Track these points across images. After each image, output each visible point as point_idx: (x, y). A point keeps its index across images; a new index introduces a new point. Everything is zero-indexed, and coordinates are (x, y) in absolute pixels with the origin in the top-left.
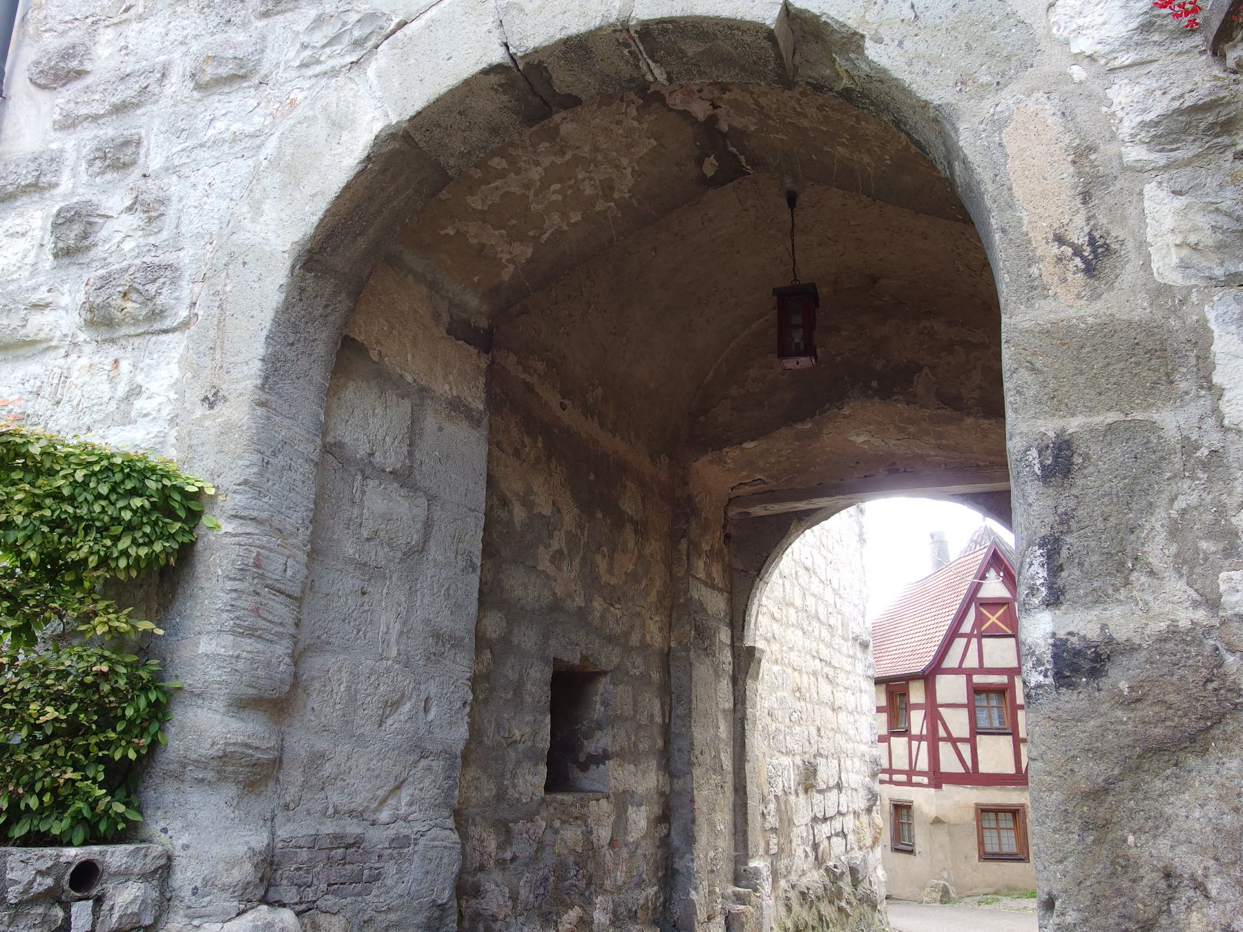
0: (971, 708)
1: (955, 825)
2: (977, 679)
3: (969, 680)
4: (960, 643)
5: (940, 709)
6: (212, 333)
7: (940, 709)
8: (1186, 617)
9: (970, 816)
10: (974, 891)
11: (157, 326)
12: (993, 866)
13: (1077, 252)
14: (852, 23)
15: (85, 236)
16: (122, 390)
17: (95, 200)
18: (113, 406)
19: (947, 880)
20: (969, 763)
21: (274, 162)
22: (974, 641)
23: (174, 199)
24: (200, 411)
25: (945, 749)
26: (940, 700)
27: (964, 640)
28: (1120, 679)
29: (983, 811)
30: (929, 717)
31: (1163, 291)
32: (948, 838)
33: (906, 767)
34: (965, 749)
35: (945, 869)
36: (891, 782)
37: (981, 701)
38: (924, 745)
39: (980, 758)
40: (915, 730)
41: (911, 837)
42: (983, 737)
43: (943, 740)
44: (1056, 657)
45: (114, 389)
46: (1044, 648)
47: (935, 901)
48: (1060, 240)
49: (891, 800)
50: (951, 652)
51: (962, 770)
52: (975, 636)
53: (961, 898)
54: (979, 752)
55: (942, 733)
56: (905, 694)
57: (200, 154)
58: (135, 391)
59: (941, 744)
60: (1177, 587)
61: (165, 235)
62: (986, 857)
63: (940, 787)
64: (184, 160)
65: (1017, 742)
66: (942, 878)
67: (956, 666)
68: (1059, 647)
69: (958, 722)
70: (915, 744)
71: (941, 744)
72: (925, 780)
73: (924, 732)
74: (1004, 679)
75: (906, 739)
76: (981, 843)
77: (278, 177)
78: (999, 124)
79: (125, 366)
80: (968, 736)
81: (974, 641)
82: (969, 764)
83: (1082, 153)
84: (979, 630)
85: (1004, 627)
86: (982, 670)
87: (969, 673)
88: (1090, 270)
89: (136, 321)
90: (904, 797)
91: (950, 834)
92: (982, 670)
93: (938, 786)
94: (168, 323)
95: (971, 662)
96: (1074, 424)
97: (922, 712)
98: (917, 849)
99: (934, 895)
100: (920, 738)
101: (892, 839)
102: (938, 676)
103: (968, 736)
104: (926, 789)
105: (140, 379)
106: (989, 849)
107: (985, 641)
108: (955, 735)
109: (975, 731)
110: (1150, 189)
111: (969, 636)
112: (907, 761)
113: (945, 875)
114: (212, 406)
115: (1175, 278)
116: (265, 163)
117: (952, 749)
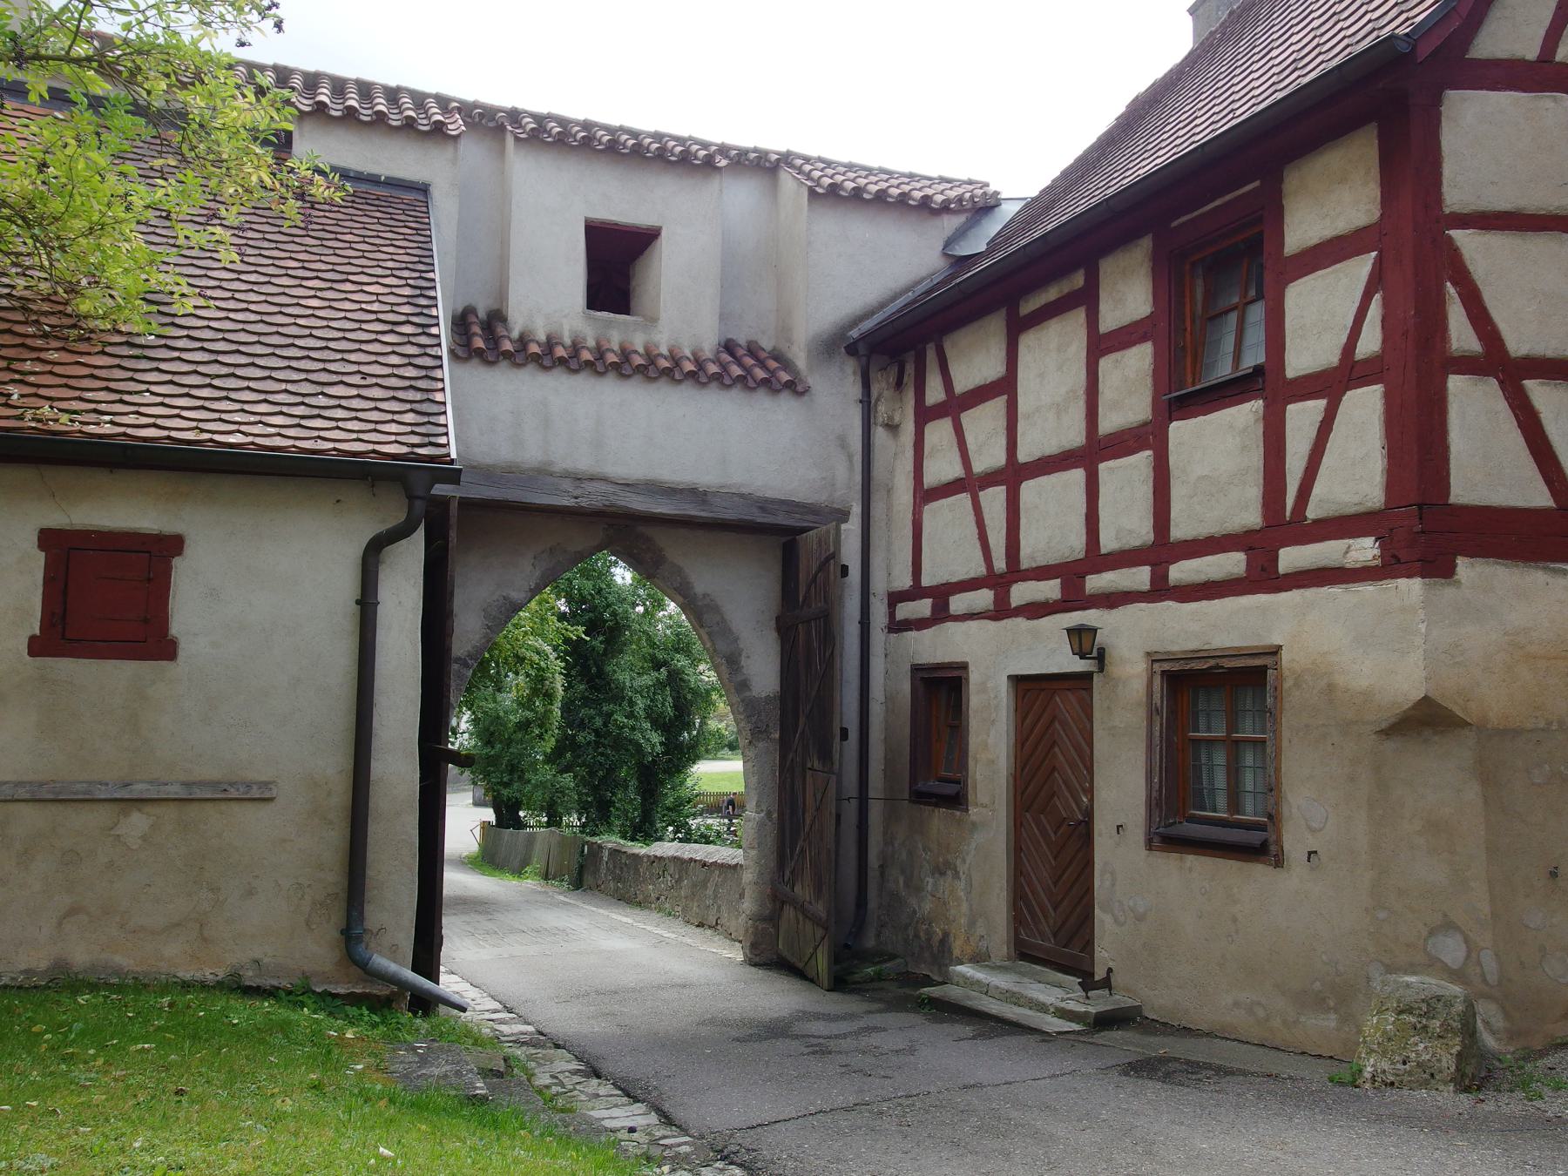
1: (1509, 733)
5: (1456, 234)
26: (1457, 194)
32: (1473, 792)
35: (1448, 926)
41: (1273, 789)
43: (1467, 365)
47: (1428, 1076)
49: (1153, 658)
53: (1529, 1055)
55: (1461, 335)
59: (1456, 384)
63: (1445, 571)
66: (1432, 964)
67: (1531, 52)
71: (1456, 384)
91: (1488, 776)
93: (1437, 567)
98: (1294, 841)
99: (1421, 1049)
101: (1153, 805)
102: (1452, 97)
104: (1368, 590)
108: (1518, 344)
113: (1452, 951)
117: (1502, 406)
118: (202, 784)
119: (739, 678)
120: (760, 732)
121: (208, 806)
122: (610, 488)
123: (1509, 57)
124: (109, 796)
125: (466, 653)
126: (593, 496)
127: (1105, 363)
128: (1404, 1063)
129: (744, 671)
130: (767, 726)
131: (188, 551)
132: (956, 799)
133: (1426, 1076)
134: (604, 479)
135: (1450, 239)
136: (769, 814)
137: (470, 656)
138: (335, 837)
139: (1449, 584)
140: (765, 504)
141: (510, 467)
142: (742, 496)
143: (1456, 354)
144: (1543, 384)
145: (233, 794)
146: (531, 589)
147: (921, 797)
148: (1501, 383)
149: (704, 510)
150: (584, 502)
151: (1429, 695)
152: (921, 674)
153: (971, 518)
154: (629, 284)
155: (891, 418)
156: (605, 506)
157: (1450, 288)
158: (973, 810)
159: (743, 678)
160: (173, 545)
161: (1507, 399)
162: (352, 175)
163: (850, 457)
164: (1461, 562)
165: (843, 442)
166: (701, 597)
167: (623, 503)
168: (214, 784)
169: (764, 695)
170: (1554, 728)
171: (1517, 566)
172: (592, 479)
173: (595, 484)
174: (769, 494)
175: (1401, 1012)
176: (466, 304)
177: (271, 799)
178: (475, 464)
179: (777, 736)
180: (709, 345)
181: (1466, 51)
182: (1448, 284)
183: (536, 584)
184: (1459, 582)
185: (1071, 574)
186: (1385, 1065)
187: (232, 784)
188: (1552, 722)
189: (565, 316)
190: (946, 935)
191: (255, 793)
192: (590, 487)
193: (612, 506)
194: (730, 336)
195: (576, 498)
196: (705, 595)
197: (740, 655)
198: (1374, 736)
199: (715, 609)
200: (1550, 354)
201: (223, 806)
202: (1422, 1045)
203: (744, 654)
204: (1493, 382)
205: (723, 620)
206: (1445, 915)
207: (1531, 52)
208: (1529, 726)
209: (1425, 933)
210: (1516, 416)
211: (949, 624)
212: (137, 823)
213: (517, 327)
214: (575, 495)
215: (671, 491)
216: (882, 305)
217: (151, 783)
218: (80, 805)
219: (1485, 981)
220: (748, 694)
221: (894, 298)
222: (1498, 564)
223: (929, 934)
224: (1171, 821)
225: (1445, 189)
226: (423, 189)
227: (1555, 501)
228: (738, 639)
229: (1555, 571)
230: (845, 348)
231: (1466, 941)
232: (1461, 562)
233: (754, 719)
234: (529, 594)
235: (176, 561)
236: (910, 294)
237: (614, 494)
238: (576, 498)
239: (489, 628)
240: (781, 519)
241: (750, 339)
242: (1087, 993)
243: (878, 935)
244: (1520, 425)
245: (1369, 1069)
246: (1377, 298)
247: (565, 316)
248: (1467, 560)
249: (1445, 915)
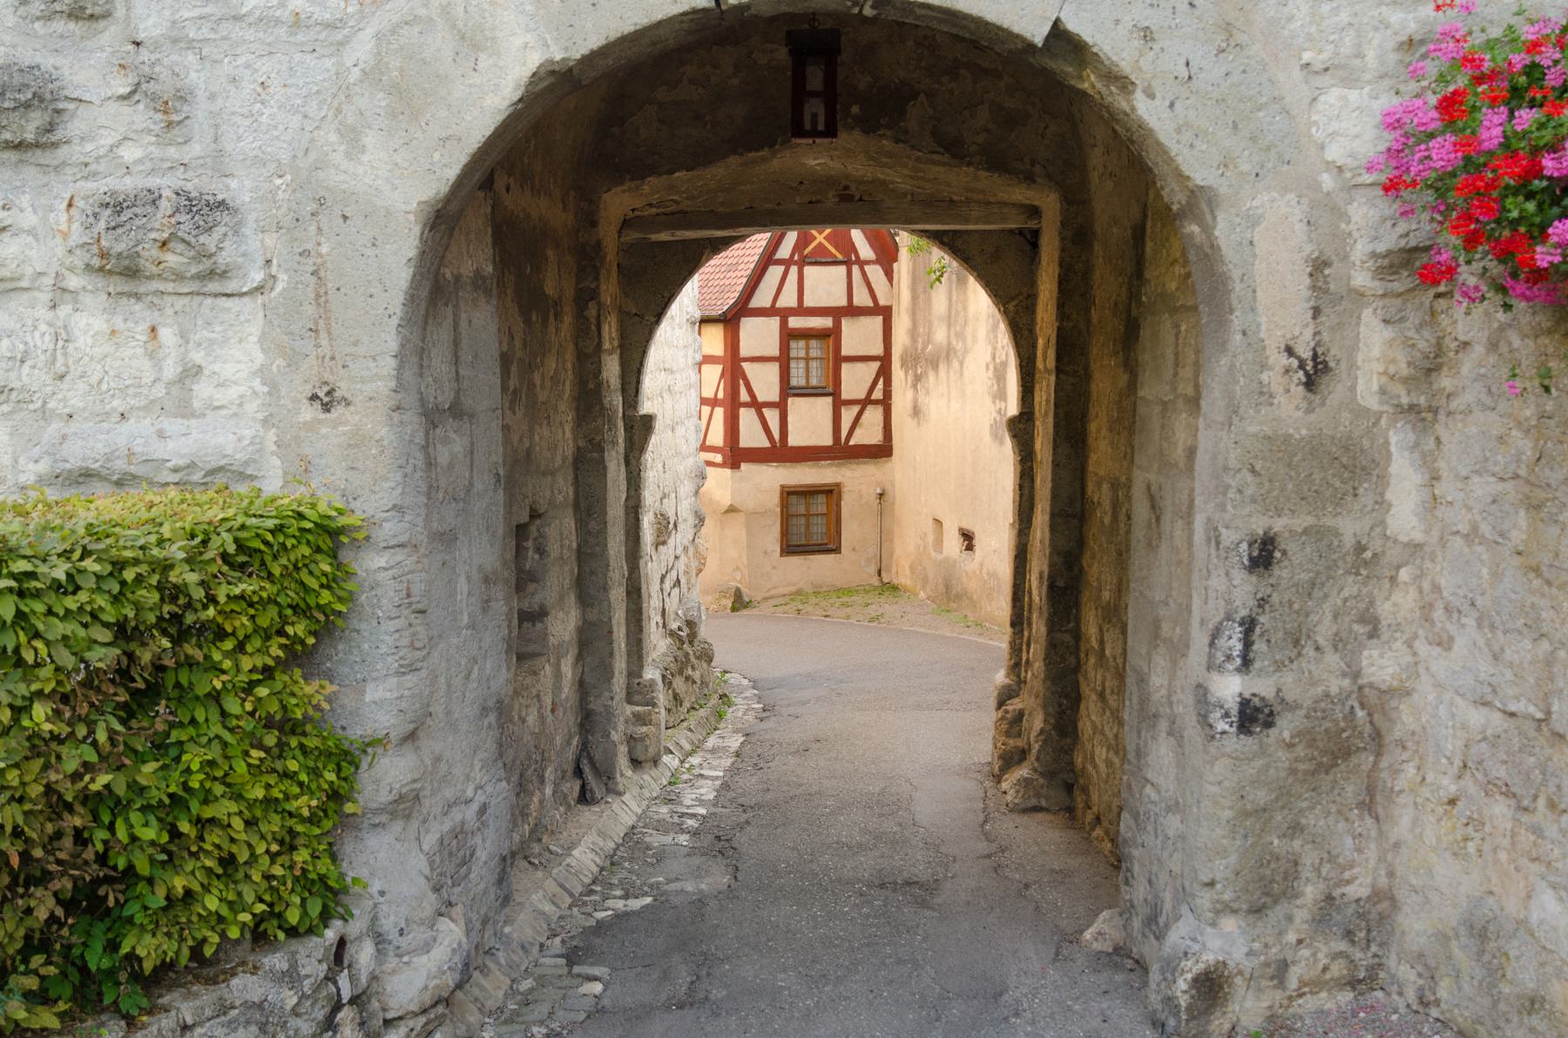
0: (784, 360)
2: (795, 322)
3: (784, 324)
4: (775, 272)
6: (310, 310)
8: (1336, 685)
9: (774, 500)
10: (772, 592)
11: (213, 286)
12: (796, 561)
13: (1302, 366)
14: (1125, 66)
15: (50, 128)
16: (171, 370)
17: (47, 62)
18: (159, 391)
19: (740, 582)
20: (776, 435)
21: (373, 75)
22: (794, 270)
23: (201, 95)
24: (309, 413)
25: (747, 417)
26: (744, 352)
27: (780, 269)
28: (1286, 727)
29: (789, 493)
30: (728, 375)
31: (1361, 412)
32: (744, 532)
34: (772, 416)
37: (798, 349)
38: (719, 412)
39: (790, 428)
42: (797, 399)
43: (746, 405)
44: (1242, 713)
45: (158, 366)
46: (1232, 705)
48: (1290, 351)
50: (763, 285)
51: (767, 444)
52: (795, 263)
54: (790, 419)
55: (744, 396)
57: (237, 31)
58: (191, 373)
59: (742, 411)
60: (1332, 659)
61: (195, 149)
62: (790, 548)
63: (738, 467)
64: (205, 33)
65: (839, 404)
67: (768, 305)
68: (1244, 704)
69: (765, 382)
71: (742, 411)
72: (718, 458)
73: (721, 395)
74: (827, 322)
76: (785, 533)
77: (381, 99)
78: (1254, 221)
79: (167, 335)
80: (777, 400)
81: (794, 270)
82: (776, 435)
83: (1319, 266)
84: (801, 255)
85: (833, 250)
86: (801, 310)
87: (784, 314)
88: (1310, 384)
89: (179, 277)
92: (801, 310)
93: (735, 465)
94: (231, 286)
95: (788, 299)
96: (1278, 525)
97: (718, 369)
99: (724, 602)
102: (743, 319)
103: (777, 400)
104: (719, 470)
105: (197, 357)
106: (795, 541)
107: (809, 271)
108: (761, 398)
109: (788, 390)
110: (1367, 313)
111: (787, 263)
114: (327, 407)
115: (1373, 403)
116: (356, 73)
207: (768, 305)
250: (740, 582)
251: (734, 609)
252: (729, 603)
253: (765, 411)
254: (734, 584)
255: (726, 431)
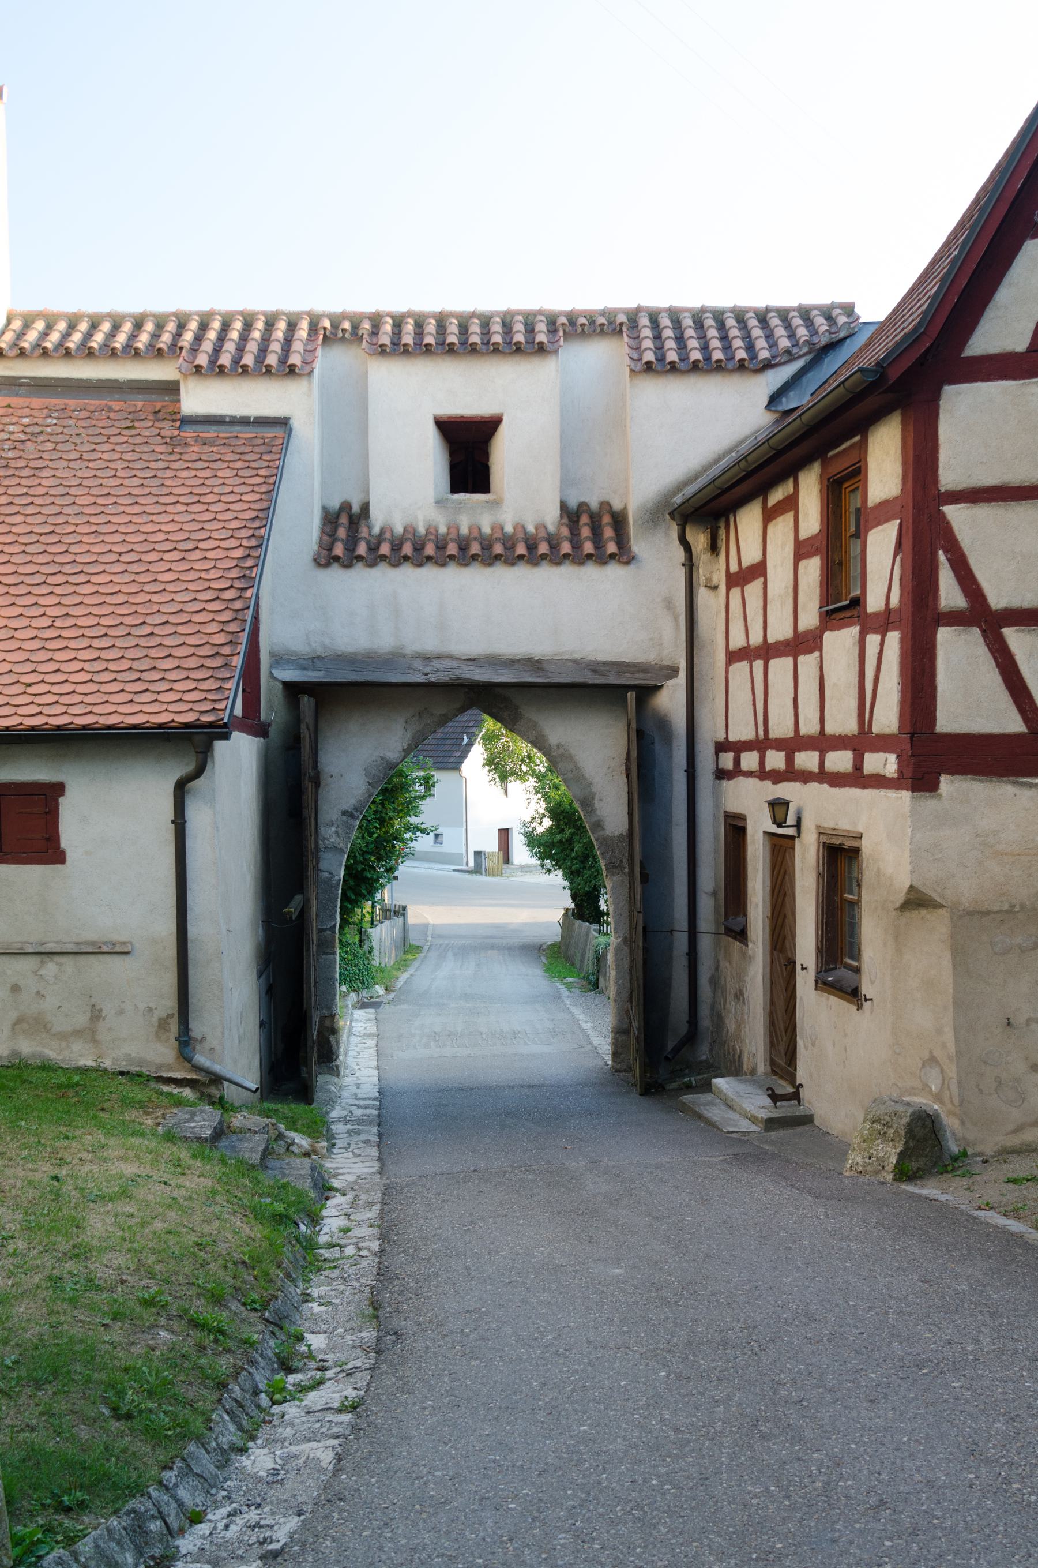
5: (950, 511)
7: (950, 511)
19: (938, 1098)
33: (851, 727)
36: (824, 776)
38: (894, 638)
40: (874, 603)
43: (955, 619)
56: (857, 473)
59: (944, 635)
70: (873, 640)
71: (944, 635)
73: (895, 601)
75: (855, 630)
90: (844, 824)
100: (884, 622)
101: (819, 951)
102: (948, 390)
104: (892, 794)
108: (997, 599)
112: (853, 703)
118: (86, 943)
119: (594, 819)
120: (614, 867)
121: (92, 958)
122: (455, 664)
123: (1001, 352)
124: (33, 951)
125: (352, 807)
126: (441, 672)
127: (802, 564)
128: (870, 1158)
129: (598, 812)
130: (621, 861)
131: (67, 792)
132: (741, 935)
133: (881, 1168)
134: (450, 657)
135: (942, 515)
136: (625, 940)
137: (356, 809)
138: (170, 978)
139: (932, 797)
140: (596, 667)
141: (369, 653)
142: (575, 661)
143: (944, 610)
144: (1018, 631)
145: (105, 949)
146: (403, 750)
147: (730, 932)
148: (983, 631)
149: (539, 677)
150: (433, 678)
151: (914, 884)
152: (729, 821)
153: (749, 685)
154: (488, 460)
155: (709, 580)
156: (451, 679)
157: (941, 556)
158: (750, 945)
159: (596, 819)
160: (58, 789)
161: (987, 645)
162: (228, 419)
163: (676, 619)
164: (944, 779)
165: (669, 604)
166: (555, 748)
167: (468, 676)
168: (93, 943)
169: (617, 834)
170: (1016, 910)
171: (991, 781)
172: (439, 657)
173: (442, 661)
174: (601, 657)
175: (873, 1122)
176: (343, 500)
177: (127, 953)
178: (340, 653)
179: (627, 870)
180: (551, 516)
181: (962, 350)
182: (941, 552)
183: (409, 745)
184: (940, 795)
185: (792, 745)
186: (859, 1160)
187: (104, 943)
188: (1015, 906)
189: (420, 508)
190: (741, 1051)
191: (118, 949)
192: (437, 664)
193: (458, 679)
194: (582, 499)
195: (426, 675)
196: (559, 746)
197: (593, 798)
198: (894, 913)
199: (570, 758)
200: (1026, 605)
201: (100, 957)
202: (881, 1146)
203: (597, 797)
204: (976, 631)
205: (577, 768)
206: (931, 1052)
208: (996, 908)
209: (920, 1065)
210: (995, 659)
211: (741, 778)
212: (51, 967)
213: (378, 518)
214: (425, 672)
215: (511, 663)
216: (705, 469)
217: (57, 943)
218: (18, 957)
219: (952, 1102)
220: (601, 833)
221: (716, 461)
222: (975, 779)
223: (734, 1050)
224: (832, 966)
225: (941, 471)
226: (283, 423)
227: (1028, 727)
228: (591, 784)
229: (1023, 785)
230: (670, 514)
231: (942, 1071)
232: (944, 779)
233: (608, 856)
234: (403, 754)
235: (61, 800)
236: (734, 454)
237: (459, 668)
238: (426, 675)
239: (370, 784)
240: (613, 680)
241: (602, 499)
242: (775, 1104)
243: (711, 1050)
244: (998, 665)
245: (850, 1162)
246: (898, 559)
247: (420, 508)
248: (949, 777)
249: (931, 1052)
250: (938, 1098)
251: (903, 1174)
252: (890, 1153)
253: (1012, 635)
254: (921, 1101)
255: (903, 692)
